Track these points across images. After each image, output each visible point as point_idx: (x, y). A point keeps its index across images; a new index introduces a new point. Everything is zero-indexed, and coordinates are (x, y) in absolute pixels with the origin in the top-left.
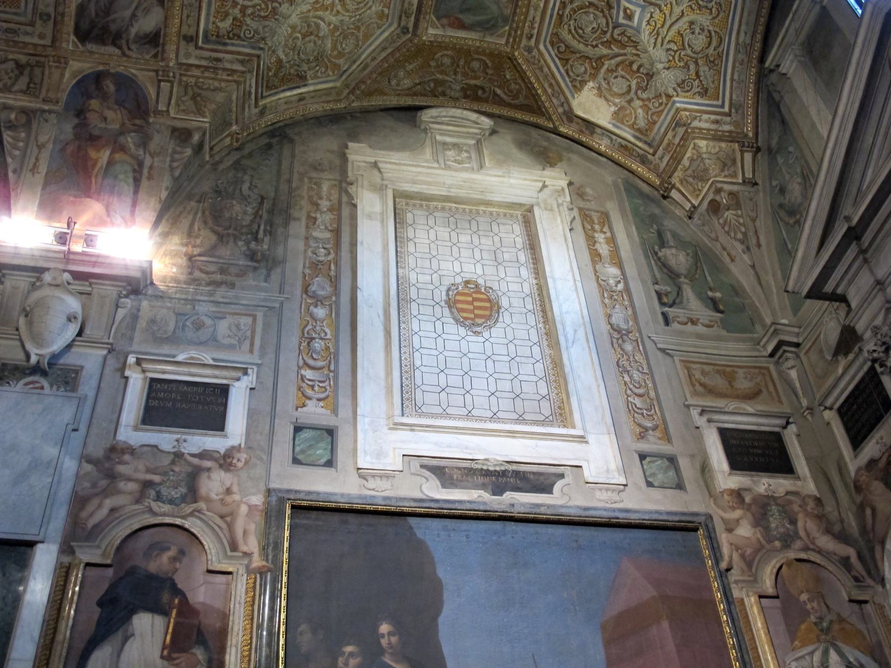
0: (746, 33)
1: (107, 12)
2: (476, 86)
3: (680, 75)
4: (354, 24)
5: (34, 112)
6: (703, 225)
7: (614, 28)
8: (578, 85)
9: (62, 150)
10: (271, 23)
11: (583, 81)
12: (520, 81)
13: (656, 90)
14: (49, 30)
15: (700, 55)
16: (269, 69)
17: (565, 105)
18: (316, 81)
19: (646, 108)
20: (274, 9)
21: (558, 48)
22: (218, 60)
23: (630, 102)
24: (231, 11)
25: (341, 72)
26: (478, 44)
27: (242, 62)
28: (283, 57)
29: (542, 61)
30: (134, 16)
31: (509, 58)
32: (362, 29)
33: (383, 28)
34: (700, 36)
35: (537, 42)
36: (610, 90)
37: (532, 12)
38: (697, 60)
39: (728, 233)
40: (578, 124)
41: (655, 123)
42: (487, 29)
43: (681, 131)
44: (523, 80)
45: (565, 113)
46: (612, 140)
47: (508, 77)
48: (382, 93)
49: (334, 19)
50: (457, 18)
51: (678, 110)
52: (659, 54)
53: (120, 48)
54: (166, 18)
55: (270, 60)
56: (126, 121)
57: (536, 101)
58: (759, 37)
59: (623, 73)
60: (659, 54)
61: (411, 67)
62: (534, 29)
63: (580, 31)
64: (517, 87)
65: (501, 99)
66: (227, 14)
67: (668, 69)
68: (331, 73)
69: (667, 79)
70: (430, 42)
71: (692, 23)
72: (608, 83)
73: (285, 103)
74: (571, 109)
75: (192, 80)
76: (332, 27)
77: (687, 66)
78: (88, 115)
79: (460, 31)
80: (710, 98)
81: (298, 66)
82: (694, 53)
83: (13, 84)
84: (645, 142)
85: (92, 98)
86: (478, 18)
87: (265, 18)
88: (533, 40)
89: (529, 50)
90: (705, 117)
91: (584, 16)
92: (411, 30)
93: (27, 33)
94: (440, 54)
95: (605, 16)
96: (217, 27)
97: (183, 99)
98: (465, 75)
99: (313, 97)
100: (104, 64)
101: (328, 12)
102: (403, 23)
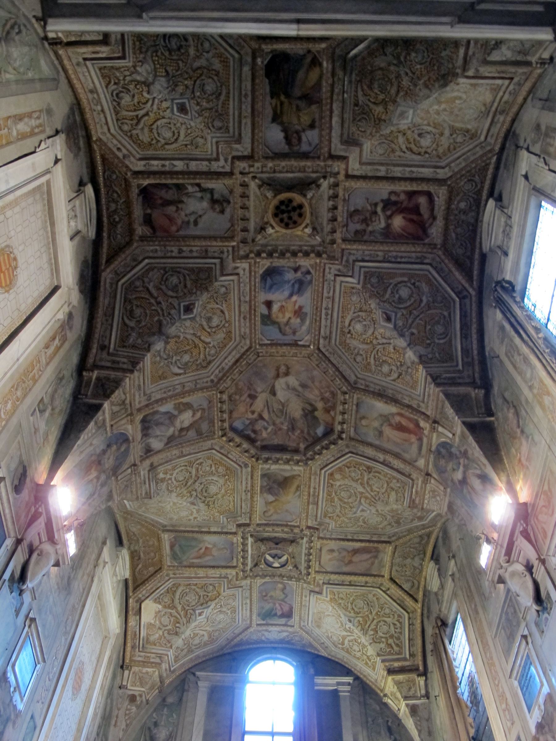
5: (105, 426)
6: (121, 697)
9: (92, 455)
10: (166, 492)
12: (149, 574)
14: (143, 404)
19: (160, 637)
20: (173, 491)
22: (145, 483)
23: (159, 628)
27: (146, 493)
30: (157, 436)
31: (160, 568)
35: (174, 578)
36: (161, 617)
39: (126, 715)
41: (155, 645)
43: (158, 660)
45: (140, 598)
51: (167, 655)
52: (188, 633)
53: (142, 439)
54: (159, 451)
58: (204, 659)
60: (188, 633)
65: (136, 568)
69: (179, 642)
74: (143, 601)
75: (134, 479)
78: (109, 451)
83: (115, 405)
84: (143, 644)
86: (178, 552)
87: (168, 489)
89: (167, 575)
90: (167, 665)
91: (193, 595)
93: (140, 395)
100: (133, 439)
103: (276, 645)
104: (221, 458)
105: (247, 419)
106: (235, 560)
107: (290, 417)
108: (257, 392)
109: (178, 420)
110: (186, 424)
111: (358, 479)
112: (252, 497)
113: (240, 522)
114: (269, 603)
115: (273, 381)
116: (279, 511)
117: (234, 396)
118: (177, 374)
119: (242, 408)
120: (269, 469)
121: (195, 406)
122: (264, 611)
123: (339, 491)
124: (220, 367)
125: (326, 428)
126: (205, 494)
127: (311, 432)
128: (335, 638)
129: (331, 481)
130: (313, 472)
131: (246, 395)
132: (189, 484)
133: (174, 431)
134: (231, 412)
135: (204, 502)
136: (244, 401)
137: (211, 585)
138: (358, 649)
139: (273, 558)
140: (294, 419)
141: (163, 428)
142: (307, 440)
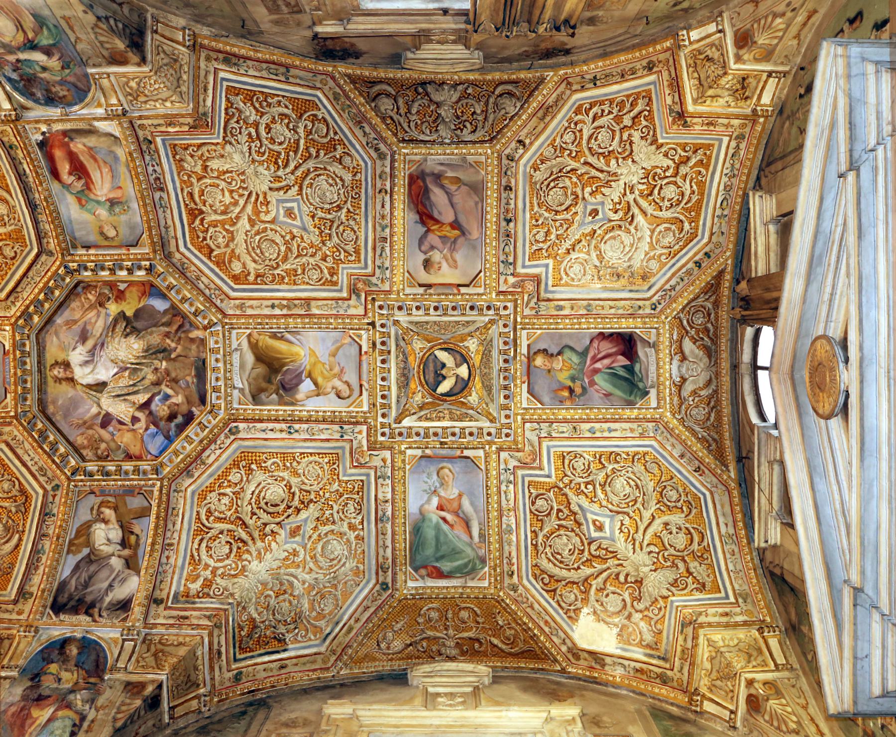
0: (726, 525)
1: (86, 585)
2: (470, 638)
3: (670, 575)
4: (330, 582)
7: (589, 544)
8: (572, 614)
11: (577, 609)
12: (513, 625)
13: (650, 596)
15: (685, 553)
16: (241, 628)
17: (567, 641)
18: (297, 645)
20: (243, 567)
21: (542, 579)
22: (186, 618)
23: (629, 617)
24: (202, 573)
25: (324, 636)
26: (460, 590)
27: (209, 618)
28: (255, 615)
29: (530, 598)
30: (111, 586)
32: (340, 587)
33: (361, 585)
34: (679, 535)
36: (606, 611)
37: (506, 548)
38: (683, 557)
40: (586, 660)
42: (468, 574)
44: (518, 624)
46: (624, 667)
47: (500, 622)
48: (374, 659)
49: (307, 577)
50: (434, 567)
52: (642, 557)
53: (91, 615)
55: (241, 617)
56: (80, 681)
57: (537, 644)
59: (613, 589)
61: (399, 626)
62: (513, 565)
63: (559, 557)
64: (513, 632)
65: (500, 649)
66: (198, 576)
67: (655, 570)
68: (312, 637)
70: (411, 595)
71: (666, 524)
72: (602, 604)
73: (264, 670)
76: (306, 585)
77: (674, 565)
79: (440, 581)
80: (710, 592)
81: (274, 628)
82: (678, 551)
85: (52, 662)
87: (235, 576)
88: (515, 576)
92: (390, 585)
94: (425, 609)
95: (577, 535)
96: (189, 588)
97: (145, 655)
98: (457, 629)
99: (296, 665)
101: (301, 570)
102: (381, 579)
103: (725, 365)
104: (211, 475)
105: (146, 429)
106: (466, 453)
107: (145, 357)
108: (99, 413)
109: (102, 548)
110: (116, 534)
111: (227, 230)
112: (300, 421)
113: (365, 442)
114: (592, 383)
115: (79, 387)
116: (337, 370)
117: (99, 452)
118: (17, 546)
119: (126, 439)
120: (242, 390)
121: (89, 517)
122: (618, 392)
123: (267, 262)
124: (36, 473)
125: (151, 295)
126: (282, 507)
127: (164, 320)
128: (669, 239)
129: (251, 278)
130: (238, 312)
131: (102, 432)
132: (244, 536)
133: (119, 556)
134: (129, 457)
135: (298, 511)
136: (113, 435)
137: (533, 503)
138: (672, 188)
139: (444, 378)
140: (146, 351)
141: (103, 574)
142: (180, 327)
